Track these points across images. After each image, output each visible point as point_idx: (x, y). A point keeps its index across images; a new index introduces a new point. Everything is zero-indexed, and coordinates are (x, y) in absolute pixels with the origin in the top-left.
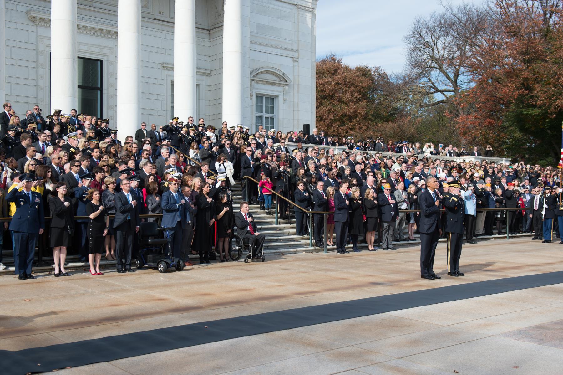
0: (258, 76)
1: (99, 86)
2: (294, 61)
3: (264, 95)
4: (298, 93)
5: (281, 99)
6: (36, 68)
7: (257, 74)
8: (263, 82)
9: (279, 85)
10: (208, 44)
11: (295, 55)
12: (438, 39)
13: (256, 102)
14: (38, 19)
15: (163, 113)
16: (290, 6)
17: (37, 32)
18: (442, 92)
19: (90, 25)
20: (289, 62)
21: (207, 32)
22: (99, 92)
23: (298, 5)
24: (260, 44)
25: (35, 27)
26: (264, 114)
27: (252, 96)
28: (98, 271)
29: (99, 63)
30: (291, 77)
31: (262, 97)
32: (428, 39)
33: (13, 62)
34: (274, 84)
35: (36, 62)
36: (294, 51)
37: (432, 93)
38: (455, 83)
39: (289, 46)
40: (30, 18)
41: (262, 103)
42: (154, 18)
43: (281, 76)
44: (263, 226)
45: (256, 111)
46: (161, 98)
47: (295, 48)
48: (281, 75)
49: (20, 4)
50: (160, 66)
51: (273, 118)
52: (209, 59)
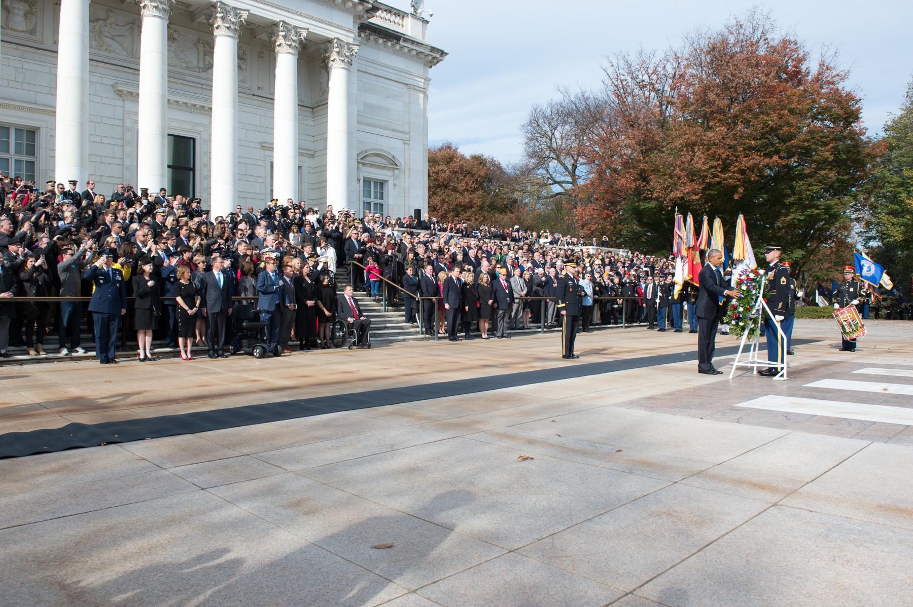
0: (366, 159)
1: (192, 166)
2: (404, 143)
3: (373, 179)
4: (409, 177)
5: (391, 183)
6: (123, 146)
7: (365, 157)
8: (371, 165)
9: (388, 168)
10: (311, 123)
11: (406, 137)
12: (555, 129)
13: (364, 187)
14: (125, 92)
15: (262, 197)
16: (400, 86)
17: (124, 107)
18: (560, 183)
19: (182, 100)
20: (399, 144)
21: (311, 110)
22: (192, 172)
25: (122, 102)
27: (359, 180)
28: (189, 356)
29: (192, 140)
31: (370, 182)
32: (546, 128)
33: (98, 139)
34: (384, 168)
35: (123, 139)
36: (405, 133)
37: (550, 184)
38: (573, 174)
39: (399, 128)
40: (117, 92)
41: (370, 188)
42: (252, 93)
44: (369, 314)
45: (364, 196)
46: (260, 180)
47: (406, 130)
49: (106, 76)
50: (258, 146)
51: (382, 205)
52: (312, 139)
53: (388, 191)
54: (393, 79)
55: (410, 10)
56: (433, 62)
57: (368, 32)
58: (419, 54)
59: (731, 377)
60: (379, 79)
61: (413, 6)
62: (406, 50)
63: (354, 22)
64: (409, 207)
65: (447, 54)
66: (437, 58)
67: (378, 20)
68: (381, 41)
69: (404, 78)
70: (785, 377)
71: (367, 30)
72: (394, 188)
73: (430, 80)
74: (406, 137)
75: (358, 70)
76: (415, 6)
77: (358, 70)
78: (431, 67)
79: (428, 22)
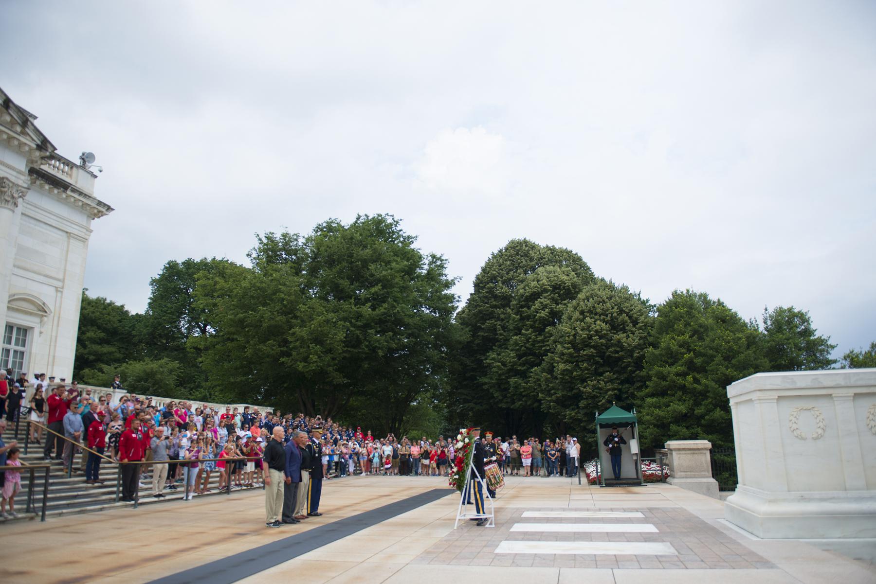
0: (11, 303)
2: (57, 291)
4: (58, 325)
8: (17, 310)
11: (60, 284)
16: (60, 233)
23: (70, 233)
24: (19, 267)
26: (13, 347)
30: (52, 308)
34: (31, 314)
41: (11, 333)
43: (40, 305)
45: (4, 342)
47: (61, 277)
53: (32, 338)
54: (54, 225)
55: (78, 162)
56: (99, 214)
57: (35, 176)
58: (85, 206)
59: (455, 528)
60: (38, 223)
61: (83, 159)
62: (72, 200)
63: (26, 165)
65: (113, 210)
66: (102, 212)
67: (45, 167)
68: (47, 187)
69: (64, 226)
70: (493, 526)
71: (35, 173)
72: (40, 336)
73: (91, 231)
74: (60, 284)
75: (22, 214)
76: (86, 159)
77: (22, 214)
78: (94, 219)
79: (96, 177)
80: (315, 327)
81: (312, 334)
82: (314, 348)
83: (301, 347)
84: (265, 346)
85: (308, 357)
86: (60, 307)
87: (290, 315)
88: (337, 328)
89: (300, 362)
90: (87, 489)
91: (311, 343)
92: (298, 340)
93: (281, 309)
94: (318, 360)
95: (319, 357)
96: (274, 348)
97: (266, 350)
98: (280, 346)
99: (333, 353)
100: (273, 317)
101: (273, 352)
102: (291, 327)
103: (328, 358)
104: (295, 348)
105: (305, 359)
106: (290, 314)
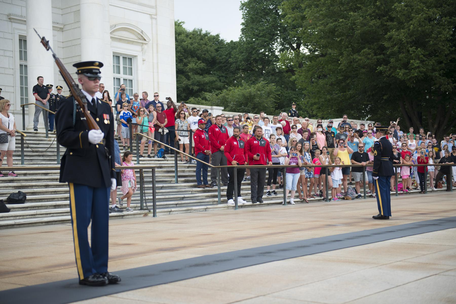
0: (114, 33)
2: (152, 18)
3: (121, 54)
4: (157, 52)
5: (140, 59)
7: (114, 31)
8: (120, 40)
11: (153, 11)
26: (122, 76)
30: (150, 35)
31: (119, 57)
36: (151, 7)
41: (119, 63)
43: (139, 34)
45: (114, 72)
47: (153, 4)
48: (140, 33)
51: (131, 81)
52: (60, 12)
64: (158, 82)
72: (143, 64)
74: (153, 11)
80: (414, 28)
81: (411, 36)
82: (414, 52)
83: (400, 52)
84: (360, 56)
85: (408, 63)
86: (157, 34)
87: (385, 18)
88: (442, 25)
89: (400, 69)
90: (192, 192)
91: (411, 47)
92: (395, 45)
93: (374, 12)
94: (421, 65)
95: (422, 61)
96: (370, 56)
97: (360, 60)
98: (376, 54)
99: (437, 56)
100: (365, 22)
101: (368, 61)
102: (387, 30)
103: (432, 62)
104: (393, 54)
105: (406, 66)
106: (384, 16)
